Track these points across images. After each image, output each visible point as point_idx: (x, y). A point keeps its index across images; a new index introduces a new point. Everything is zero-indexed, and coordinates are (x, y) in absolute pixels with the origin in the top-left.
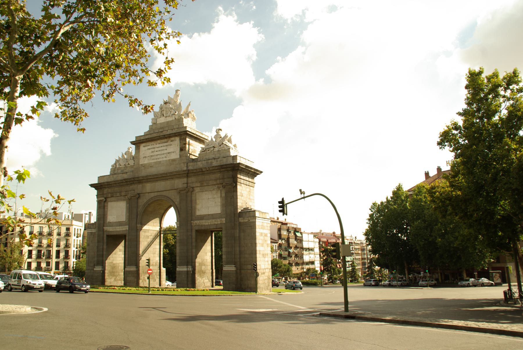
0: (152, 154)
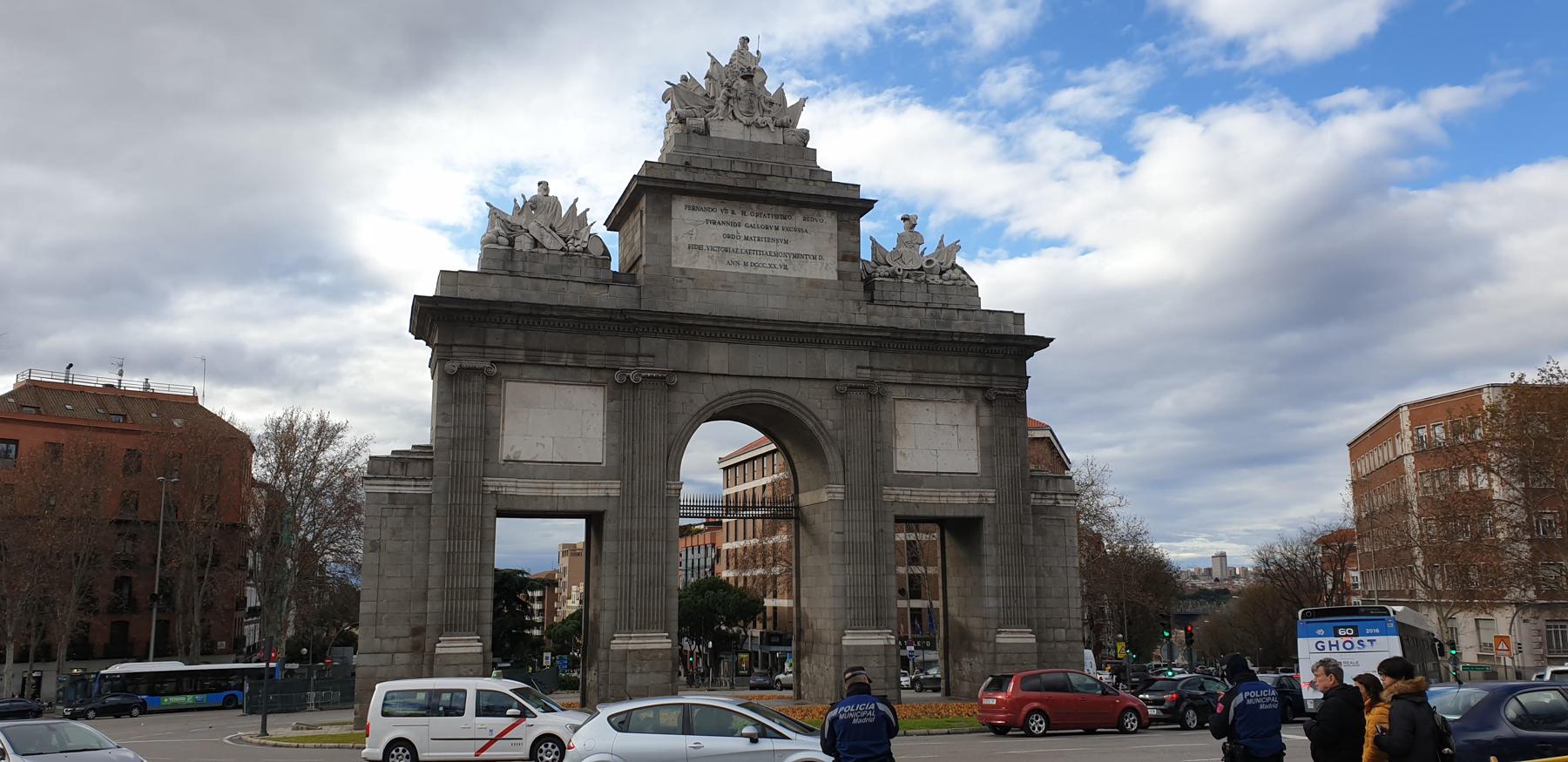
0: (727, 243)
